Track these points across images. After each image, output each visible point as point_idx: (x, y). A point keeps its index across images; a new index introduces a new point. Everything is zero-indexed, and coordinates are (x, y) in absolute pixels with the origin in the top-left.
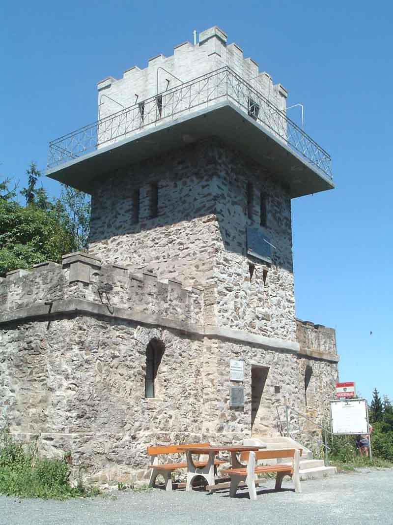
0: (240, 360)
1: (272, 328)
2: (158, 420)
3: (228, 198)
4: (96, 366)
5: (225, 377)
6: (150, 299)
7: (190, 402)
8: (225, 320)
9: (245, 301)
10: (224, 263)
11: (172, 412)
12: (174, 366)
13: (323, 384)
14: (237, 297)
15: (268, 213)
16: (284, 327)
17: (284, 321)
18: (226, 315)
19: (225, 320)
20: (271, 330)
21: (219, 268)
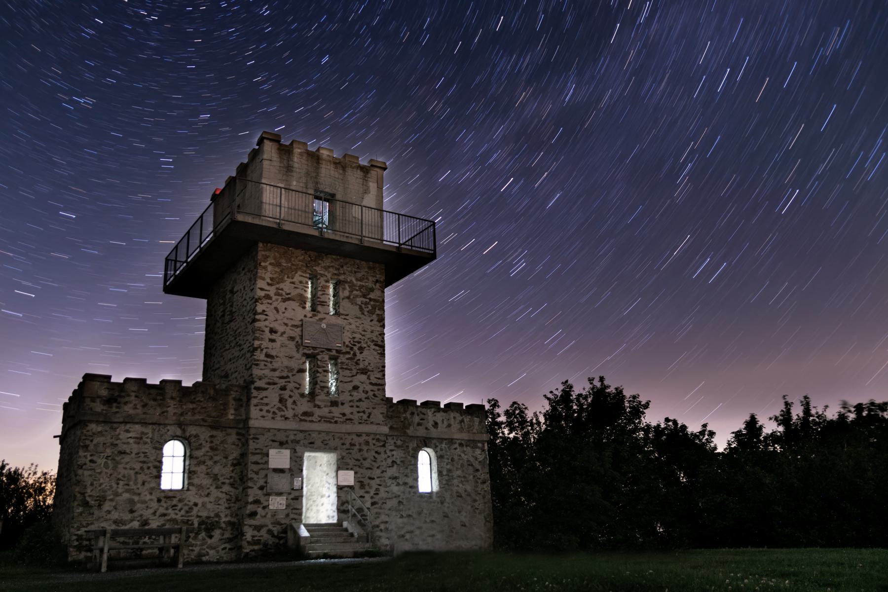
0: (286, 449)
1: (344, 415)
2: (179, 508)
3: (274, 298)
4: (103, 465)
5: (261, 466)
6: (172, 403)
7: (224, 491)
8: (264, 413)
9: (296, 391)
10: (266, 359)
11: (200, 501)
12: (202, 459)
14: (283, 388)
15: (343, 299)
16: (364, 412)
17: (363, 405)
18: (265, 408)
19: (264, 413)
20: (341, 416)
21: (257, 365)
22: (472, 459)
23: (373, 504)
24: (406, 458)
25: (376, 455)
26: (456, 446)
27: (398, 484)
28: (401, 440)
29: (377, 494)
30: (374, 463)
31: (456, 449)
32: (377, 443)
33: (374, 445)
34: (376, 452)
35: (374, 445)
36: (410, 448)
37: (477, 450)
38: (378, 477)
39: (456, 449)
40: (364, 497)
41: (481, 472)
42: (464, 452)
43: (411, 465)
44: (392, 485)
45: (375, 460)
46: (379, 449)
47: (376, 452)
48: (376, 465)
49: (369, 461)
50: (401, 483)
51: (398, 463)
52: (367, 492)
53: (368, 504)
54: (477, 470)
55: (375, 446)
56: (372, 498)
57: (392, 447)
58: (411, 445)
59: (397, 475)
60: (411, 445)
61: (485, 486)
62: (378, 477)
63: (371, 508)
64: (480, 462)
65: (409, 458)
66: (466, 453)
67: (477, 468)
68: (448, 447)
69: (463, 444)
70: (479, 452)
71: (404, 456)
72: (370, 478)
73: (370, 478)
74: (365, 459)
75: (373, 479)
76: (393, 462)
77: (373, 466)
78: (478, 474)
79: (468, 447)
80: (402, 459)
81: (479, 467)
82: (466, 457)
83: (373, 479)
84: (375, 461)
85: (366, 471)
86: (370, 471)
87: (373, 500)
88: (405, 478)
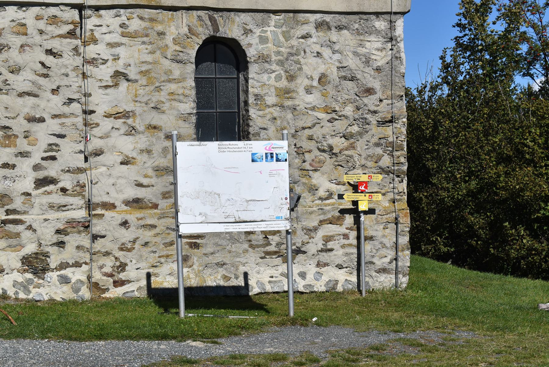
13: (302, 82)
22: (352, 62)
23: (41, 183)
24: (155, 63)
25: (50, 60)
26: (310, 28)
27: (132, 131)
28: (141, 18)
29: (53, 158)
30: (42, 81)
31: (306, 37)
32: (50, 28)
33: (41, 32)
34: (49, 52)
35: (41, 32)
36: (169, 40)
37: (372, 38)
38: (55, 116)
39: (306, 37)
40: (13, 166)
41: (379, 95)
42: (331, 44)
43: (169, 81)
44: (115, 133)
45: (45, 71)
46: (55, 45)
47: (49, 52)
48: (47, 84)
49: (27, 75)
50: (141, 128)
51: (132, 76)
52: (23, 154)
53: (28, 184)
54: (370, 91)
55: (45, 37)
56: (36, 168)
57: (115, 38)
58: (173, 29)
59: (129, 107)
60: (173, 29)
61: (388, 131)
62: (55, 116)
63: (34, 193)
64: (378, 70)
65: (167, 63)
66: (337, 47)
67: (370, 85)
68: (283, 33)
69: (327, 23)
70: (379, 45)
71: (149, 58)
72: (31, 120)
73: (31, 120)
74: (15, 70)
75: (42, 120)
76: (117, 74)
77: (40, 87)
78: (370, 101)
79: (345, 32)
80: (144, 68)
81: (376, 85)
82: (337, 56)
83: (42, 120)
84: (46, 76)
85: (20, 100)
86: (31, 100)
87: (41, 174)
88: (154, 113)
